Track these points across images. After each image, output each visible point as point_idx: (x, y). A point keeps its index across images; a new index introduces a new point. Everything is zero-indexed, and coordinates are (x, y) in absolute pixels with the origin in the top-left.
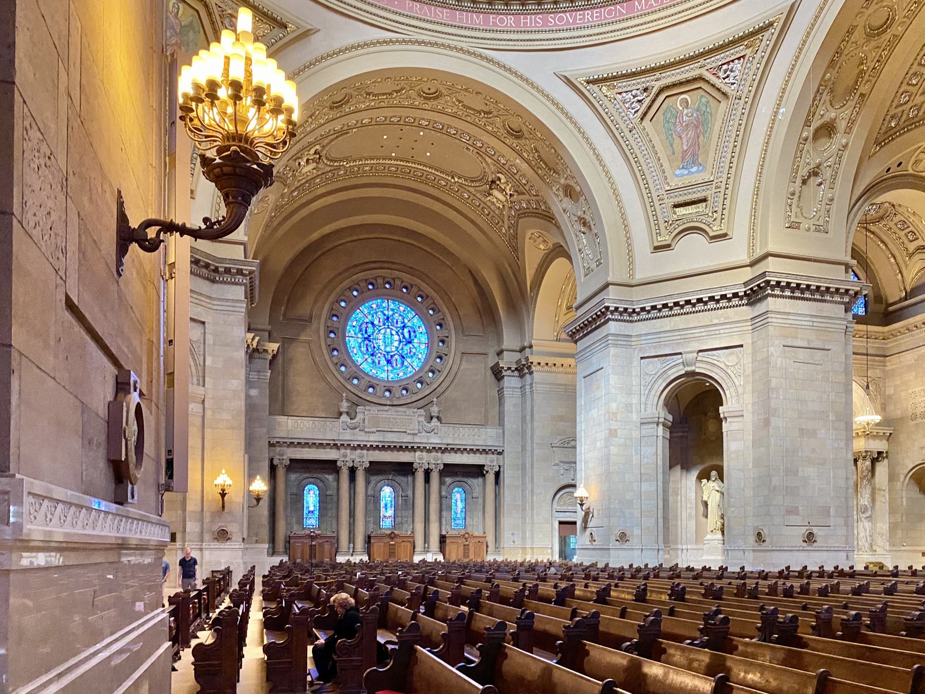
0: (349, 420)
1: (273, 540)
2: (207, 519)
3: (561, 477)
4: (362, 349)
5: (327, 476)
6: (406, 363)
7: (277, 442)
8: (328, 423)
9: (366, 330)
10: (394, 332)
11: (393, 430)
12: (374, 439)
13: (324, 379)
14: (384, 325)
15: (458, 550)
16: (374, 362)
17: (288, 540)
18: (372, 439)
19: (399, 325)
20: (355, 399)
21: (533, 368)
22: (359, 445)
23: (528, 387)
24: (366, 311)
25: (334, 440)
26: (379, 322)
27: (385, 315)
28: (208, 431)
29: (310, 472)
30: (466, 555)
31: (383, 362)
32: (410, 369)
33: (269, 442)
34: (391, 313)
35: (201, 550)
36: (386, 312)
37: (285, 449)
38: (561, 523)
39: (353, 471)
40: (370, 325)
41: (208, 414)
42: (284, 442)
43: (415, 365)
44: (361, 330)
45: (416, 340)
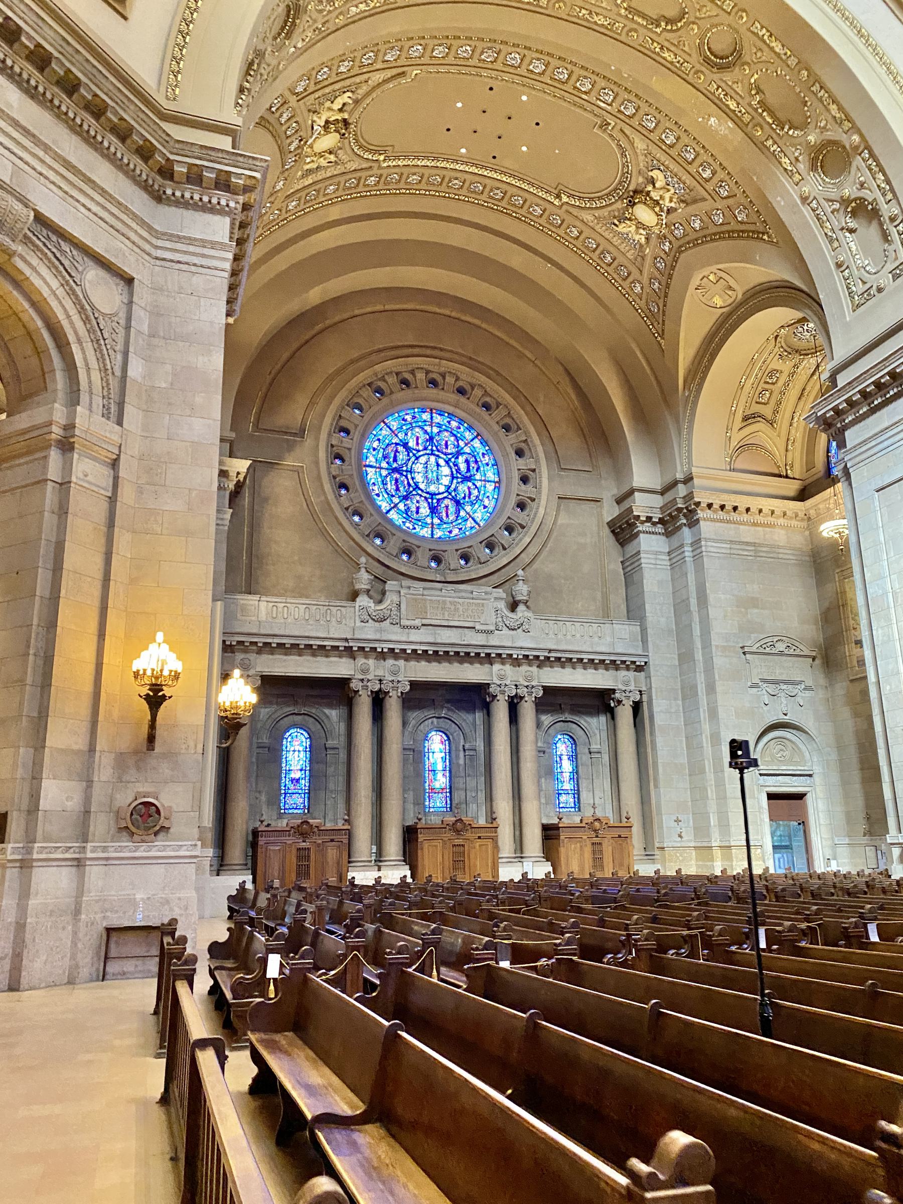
0: (372, 605)
1: (221, 840)
2: (104, 772)
3: (765, 708)
4: (389, 486)
5: (327, 711)
6: (462, 513)
7: (239, 643)
8: (334, 609)
9: (395, 456)
10: (442, 462)
11: (451, 624)
12: (420, 638)
13: (324, 533)
14: (425, 449)
15: (582, 855)
16: (408, 509)
17: (254, 840)
18: (412, 638)
19: (449, 451)
20: (379, 570)
21: (701, 514)
22: (392, 650)
23: (688, 551)
24: (394, 425)
25: (346, 640)
26: (417, 444)
27: (426, 432)
28: (123, 541)
29: (296, 703)
30: (598, 861)
31: (425, 510)
32: (470, 523)
33: (224, 641)
34: (436, 430)
35: (79, 864)
36: (428, 429)
37: (252, 656)
38: (771, 796)
39: (378, 700)
40: (400, 448)
41: (126, 494)
42: (251, 643)
43: (478, 516)
44: (385, 457)
45: (478, 477)
